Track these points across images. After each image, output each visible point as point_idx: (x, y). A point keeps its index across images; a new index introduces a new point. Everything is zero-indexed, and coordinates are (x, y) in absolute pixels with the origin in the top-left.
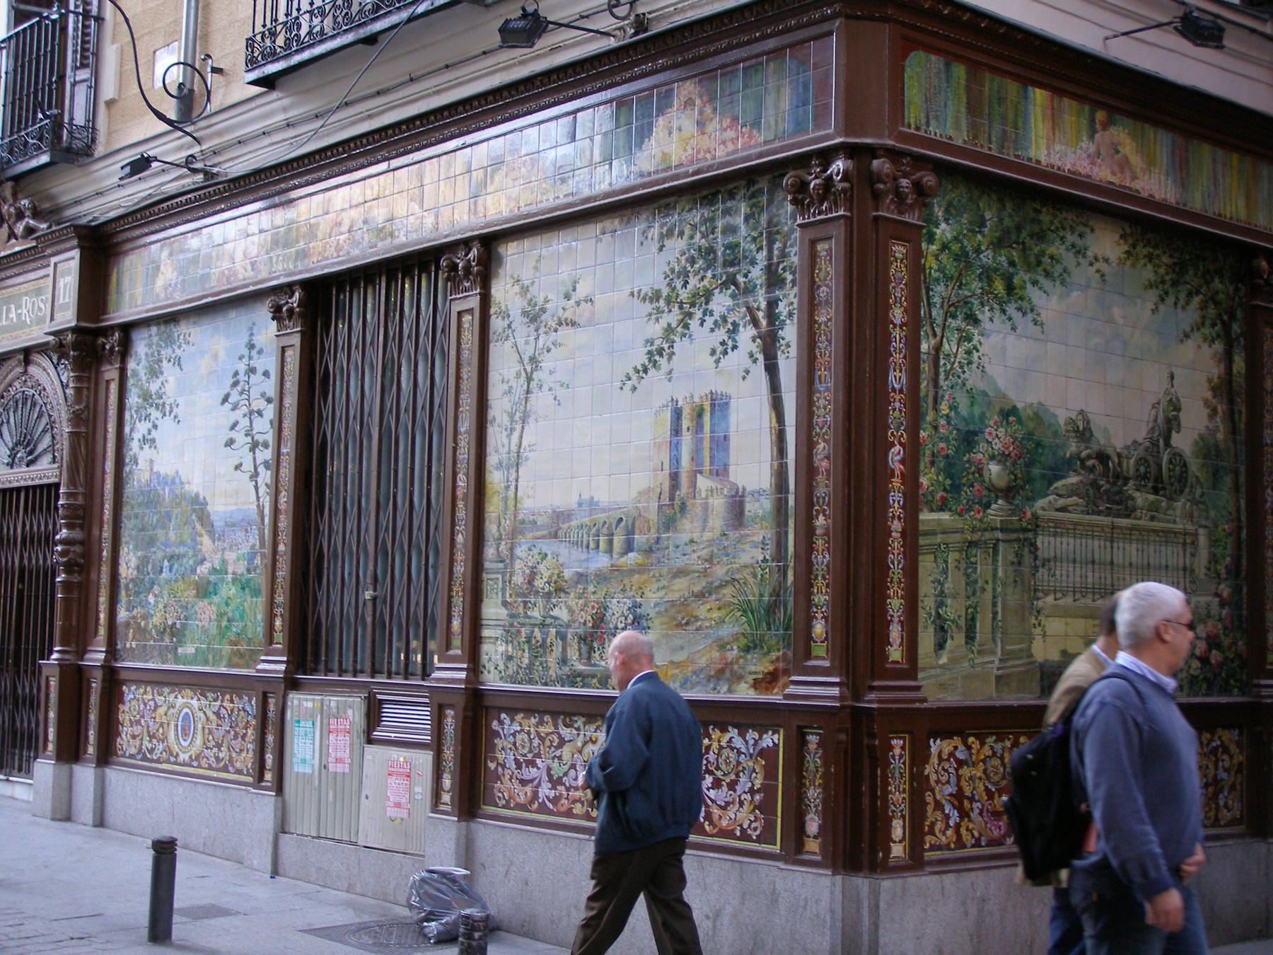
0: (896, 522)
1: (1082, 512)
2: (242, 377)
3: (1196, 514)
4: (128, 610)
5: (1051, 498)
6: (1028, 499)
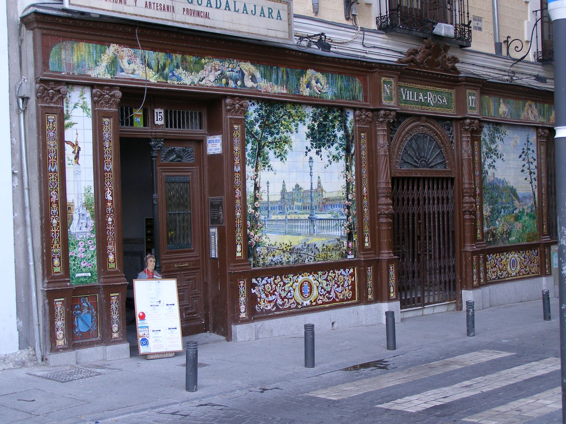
2: (525, 150)
4: (487, 227)
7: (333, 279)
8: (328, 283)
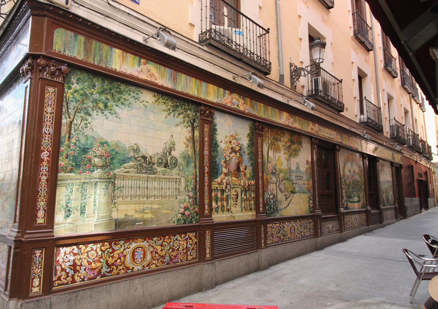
0: (44, 176)
1: (135, 173)
3: (180, 173)
5: (122, 169)
6: (112, 169)
7: (168, 244)
8: (163, 248)
